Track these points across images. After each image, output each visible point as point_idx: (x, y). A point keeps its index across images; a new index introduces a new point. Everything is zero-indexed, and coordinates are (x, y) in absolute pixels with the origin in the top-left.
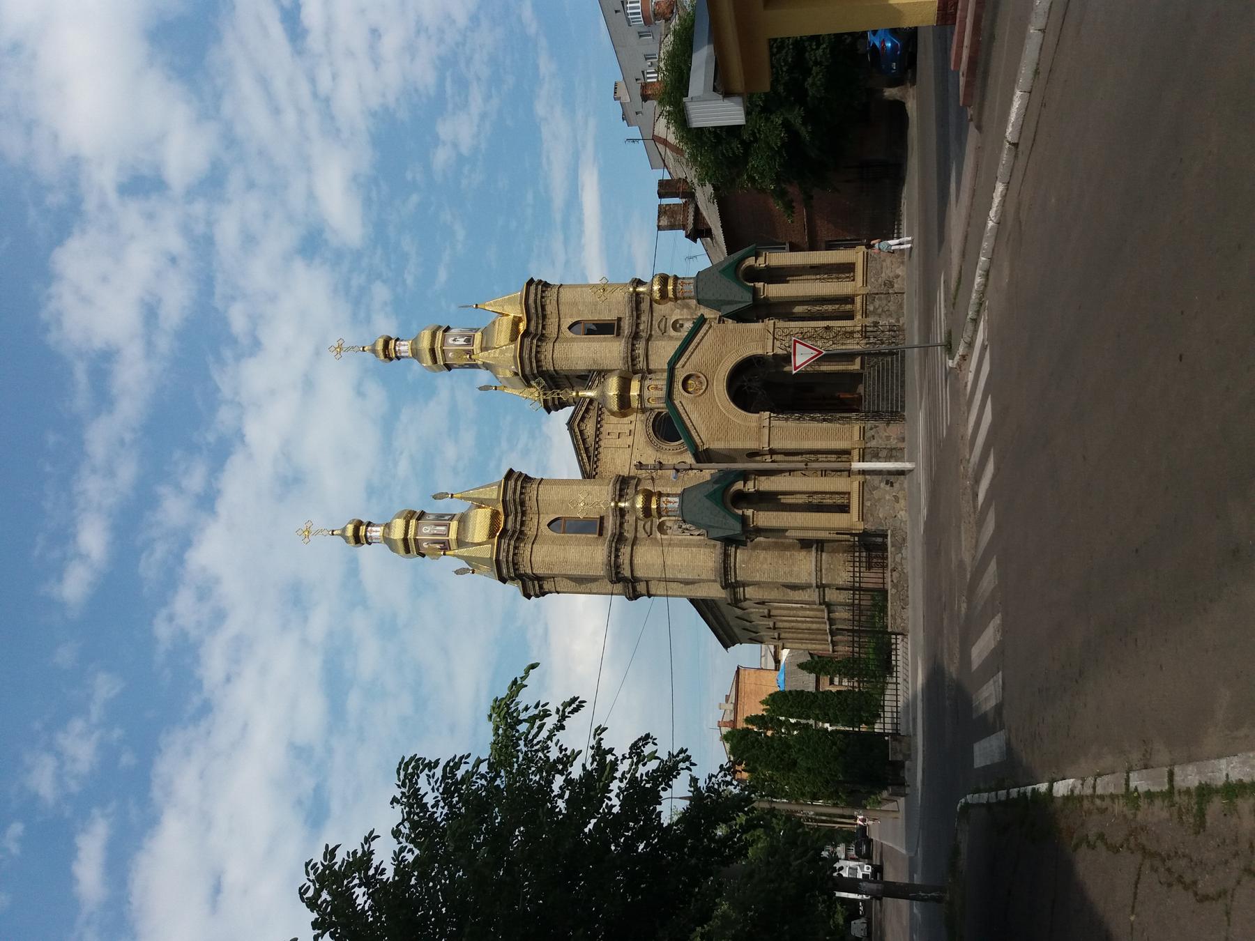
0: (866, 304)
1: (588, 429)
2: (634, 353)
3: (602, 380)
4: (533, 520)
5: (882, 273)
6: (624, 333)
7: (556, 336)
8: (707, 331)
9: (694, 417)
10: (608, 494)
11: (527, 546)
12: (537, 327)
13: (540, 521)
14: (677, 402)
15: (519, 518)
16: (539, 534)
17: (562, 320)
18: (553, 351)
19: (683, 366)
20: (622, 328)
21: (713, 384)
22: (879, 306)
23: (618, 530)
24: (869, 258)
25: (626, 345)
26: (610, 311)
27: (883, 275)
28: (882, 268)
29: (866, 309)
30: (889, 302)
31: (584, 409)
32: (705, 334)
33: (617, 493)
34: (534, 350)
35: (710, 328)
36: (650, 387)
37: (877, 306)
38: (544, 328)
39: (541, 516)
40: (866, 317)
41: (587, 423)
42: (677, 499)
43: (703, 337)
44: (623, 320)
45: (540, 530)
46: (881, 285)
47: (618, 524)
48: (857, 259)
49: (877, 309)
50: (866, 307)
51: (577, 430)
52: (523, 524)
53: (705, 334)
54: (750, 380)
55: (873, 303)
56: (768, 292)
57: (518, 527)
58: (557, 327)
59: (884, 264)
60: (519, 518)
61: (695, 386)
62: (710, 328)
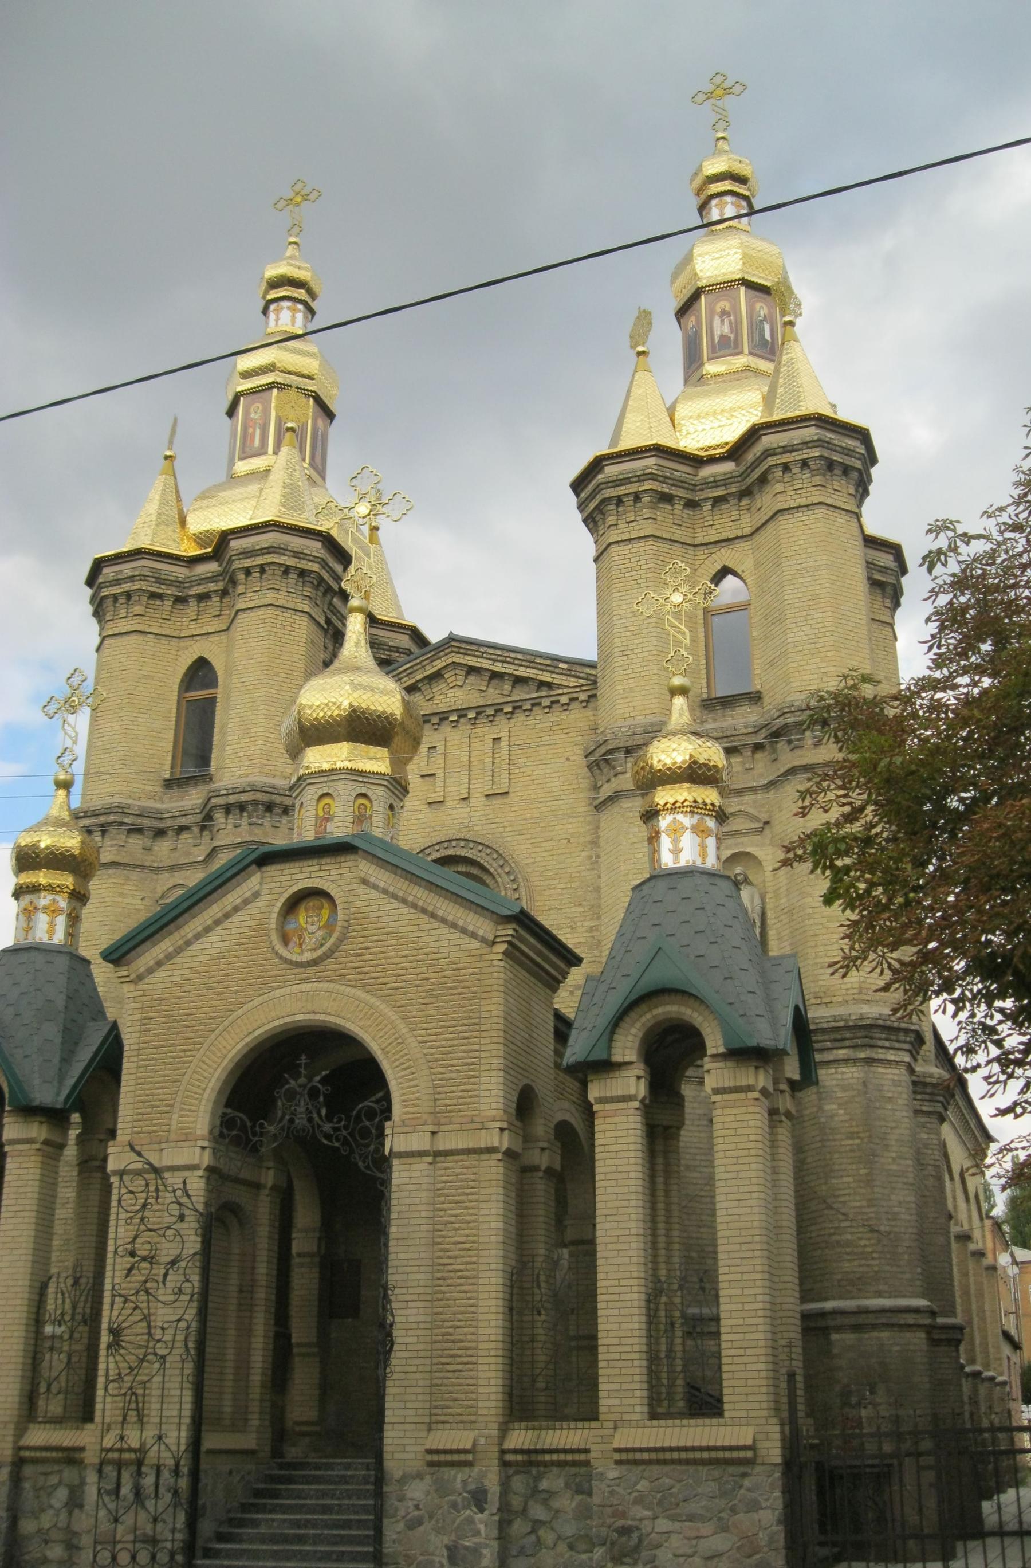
0: (561, 1464)
1: (451, 693)
2: (620, 756)
3: (583, 696)
4: (215, 621)
5: (673, 1518)
6: (715, 720)
7: (697, 541)
8: (473, 935)
9: (216, 942)
10: (240, 777)
11: (137, 619)
12: (716, 484)
13: (213, 638)
14: (254, 881)
15: (212, 587)
16: (183, 644)
17: (747, 545)
18: (630, 540)
19: (364, 882)
20: (728, 712)
21: (308, 980)
22: (557, 1511)
23: (169, 823)
24: (731, 1469)
25: (639, 730)
26: (772, 664)
27: (663, 1524)
28: (691, 1518)
29: (545, 1464)
30: (571, 1547)
31: (498, 667)
32: (464, 931)
33: (232, 799)
34: (621, 490)
35: (483, 940)
36: (326, 800)
37: (556, 1504)
38: (718, 501)
39: (223, 637)
40: (505, 1464)
41: (467, 688)
42: (59, 937)
43: (454, 925)
44: (755, 708)
45: (188, 642)
46: (623, 1515)
47: (183, 821)
48: (735, 1422)
49: (545, 1502)
50: (553, 1463)
51: (439, 664)
52: (203, 597)
53: (464, 931)
54: (314, 1093)
55: (567, 1485)
56: (615, 1113)
57: (193, 592)
58: (724, 536)
59: (706, 1529)
60: (212, 587)
61: (312, 928)
62: (483, 940)
